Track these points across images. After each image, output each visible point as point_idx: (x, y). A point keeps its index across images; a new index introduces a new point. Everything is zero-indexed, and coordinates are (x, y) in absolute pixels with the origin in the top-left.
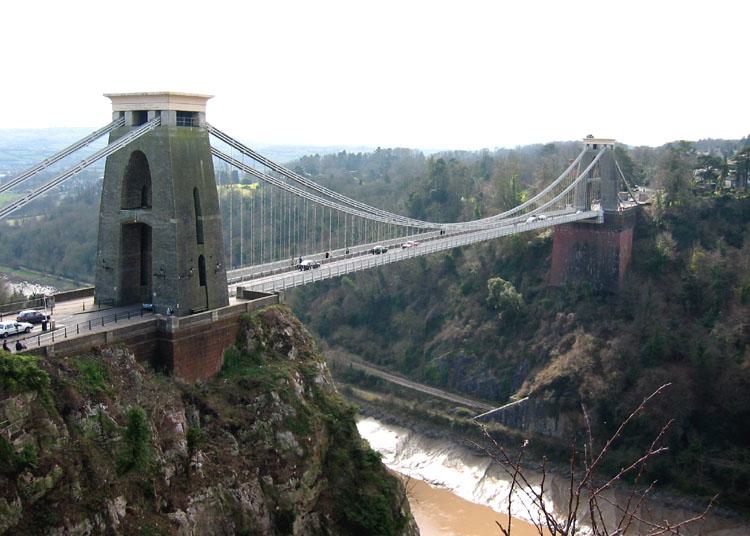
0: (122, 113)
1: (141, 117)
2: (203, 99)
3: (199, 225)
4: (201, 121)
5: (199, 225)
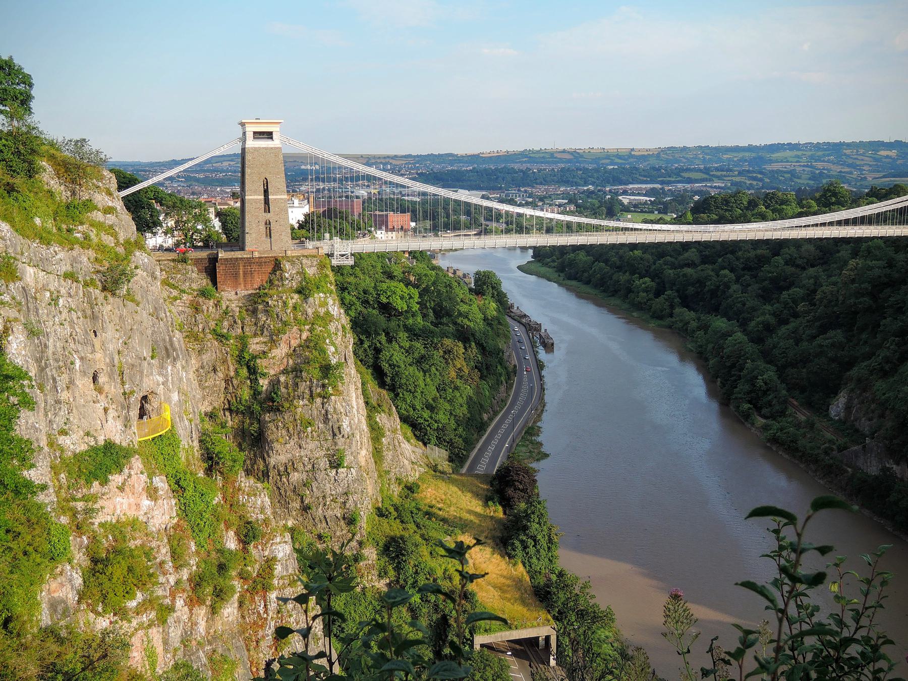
3: (267, 201)
5: (267, 201)
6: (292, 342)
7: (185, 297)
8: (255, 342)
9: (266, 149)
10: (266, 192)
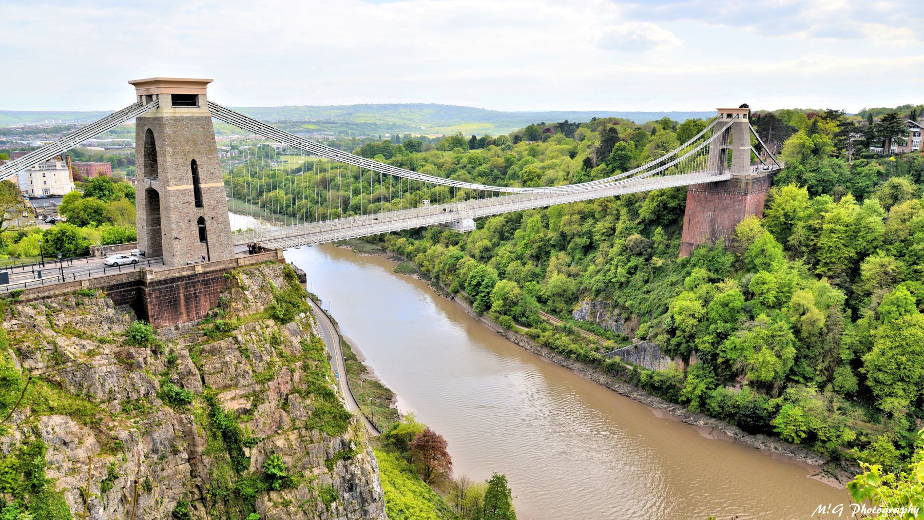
0: (141, 96)
1: (150, 97)
2: (204, 83)
4: (201, 101)
6: (283, 388)
7: (107, 349)
8: (228, 397)
9: (191, 119)
10: (196, 181)
